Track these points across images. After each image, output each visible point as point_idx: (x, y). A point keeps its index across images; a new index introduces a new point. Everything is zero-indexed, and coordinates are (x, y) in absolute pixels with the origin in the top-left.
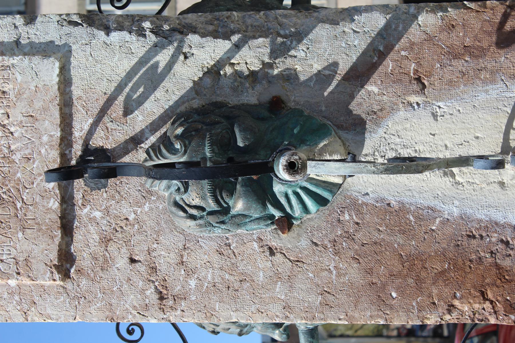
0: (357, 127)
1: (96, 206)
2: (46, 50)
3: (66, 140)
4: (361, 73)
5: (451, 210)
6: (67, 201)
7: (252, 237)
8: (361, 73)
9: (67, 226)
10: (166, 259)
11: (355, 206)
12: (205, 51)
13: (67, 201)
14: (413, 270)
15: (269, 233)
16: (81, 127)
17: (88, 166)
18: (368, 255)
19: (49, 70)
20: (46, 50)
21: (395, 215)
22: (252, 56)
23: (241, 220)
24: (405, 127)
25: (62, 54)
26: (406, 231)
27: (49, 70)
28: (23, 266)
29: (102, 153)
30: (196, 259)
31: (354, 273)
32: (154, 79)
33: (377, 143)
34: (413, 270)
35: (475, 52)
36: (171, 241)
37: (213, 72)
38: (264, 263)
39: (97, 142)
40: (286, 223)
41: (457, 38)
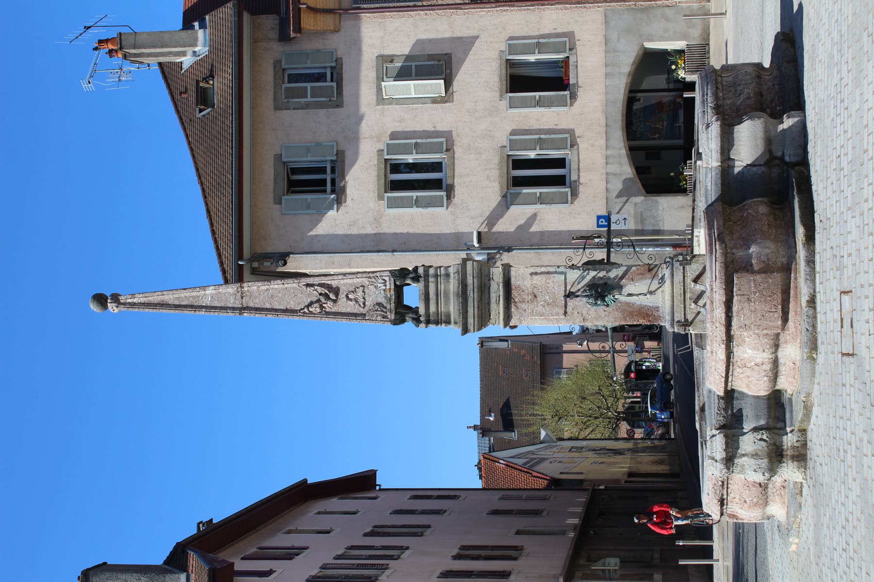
0: (621, 288)
1: (571, 303)
2: (562, 273)
3: (566, 290)
4: (622, 278)
5: (638, 303)
6: (566, 302)
7: (601, 309)
8: (622, 278)
9: (566, 307)
10: (584, 313)
11: (621, 303)
12: (593, 274)
13: (566, 302)
14: (631, 314)
15: (604, 307)
16: (568, 289)
17: (569, 295)
18: (623, 312)
19: (563, 277)
20: (562, 273)
21: (628, 304)
22: (601, 274)
23: (599, 305)
24: (630, 288)
25: (565, 274)
26: (630, 307)
27: (563, 277)
28: (557, 314)
29: (572, 293)
30: (591, 312)
31: (620, 315)
32: (583, 278)
33: (625, 291)
34: (631, 314)
35: (643, 274)
36: (586, 309)
37: (594, 277)
38: (603, 313)
39: (572, 290)
40: (608, 306)
41: (639, 271)
